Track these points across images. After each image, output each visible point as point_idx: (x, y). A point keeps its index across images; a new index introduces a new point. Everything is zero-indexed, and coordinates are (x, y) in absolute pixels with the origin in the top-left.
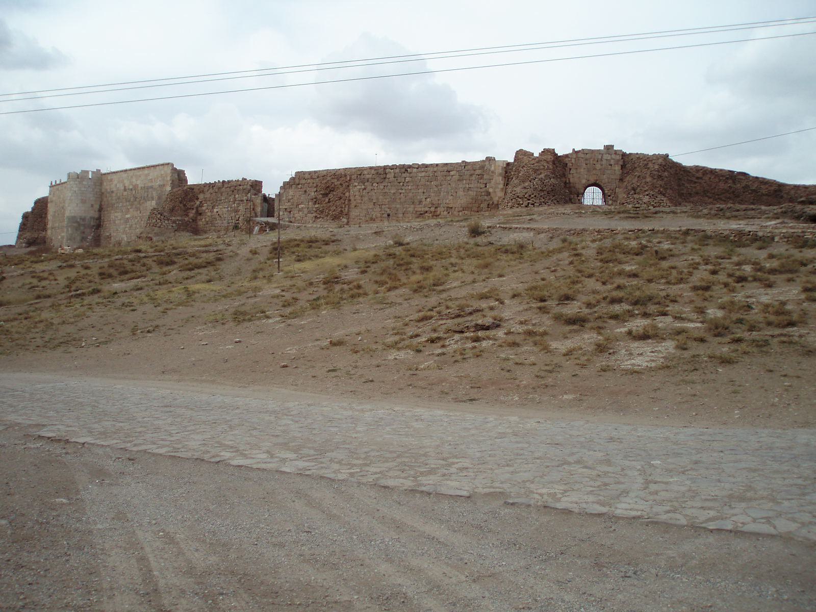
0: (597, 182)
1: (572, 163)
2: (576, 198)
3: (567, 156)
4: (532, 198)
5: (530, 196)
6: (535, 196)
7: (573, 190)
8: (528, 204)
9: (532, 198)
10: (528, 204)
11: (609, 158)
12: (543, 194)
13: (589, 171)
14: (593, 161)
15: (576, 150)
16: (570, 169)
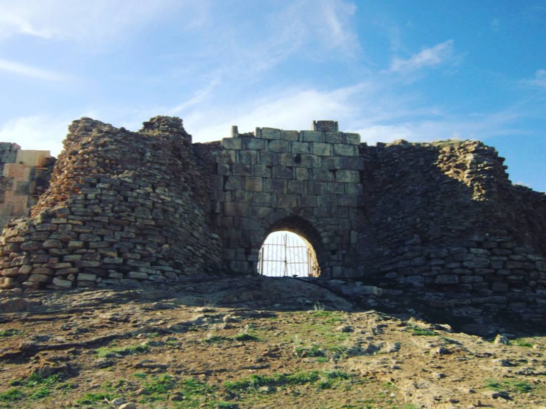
0: (301, 215)
1: (230, 163)
2: (243, 257)
3: (216, 146)
4: (73, 251)
5: (65, 243)
6: (86, 245)
7: (234, 234)
8: (53, 273)
9: (73, 251)
10: (52, 276)
11: (327, 153)
12: (118, 235)
13: (277, 184)
14: (287, 156)
15: (241, 131)
16: (226, 178)
